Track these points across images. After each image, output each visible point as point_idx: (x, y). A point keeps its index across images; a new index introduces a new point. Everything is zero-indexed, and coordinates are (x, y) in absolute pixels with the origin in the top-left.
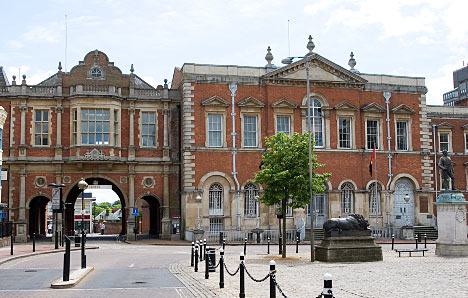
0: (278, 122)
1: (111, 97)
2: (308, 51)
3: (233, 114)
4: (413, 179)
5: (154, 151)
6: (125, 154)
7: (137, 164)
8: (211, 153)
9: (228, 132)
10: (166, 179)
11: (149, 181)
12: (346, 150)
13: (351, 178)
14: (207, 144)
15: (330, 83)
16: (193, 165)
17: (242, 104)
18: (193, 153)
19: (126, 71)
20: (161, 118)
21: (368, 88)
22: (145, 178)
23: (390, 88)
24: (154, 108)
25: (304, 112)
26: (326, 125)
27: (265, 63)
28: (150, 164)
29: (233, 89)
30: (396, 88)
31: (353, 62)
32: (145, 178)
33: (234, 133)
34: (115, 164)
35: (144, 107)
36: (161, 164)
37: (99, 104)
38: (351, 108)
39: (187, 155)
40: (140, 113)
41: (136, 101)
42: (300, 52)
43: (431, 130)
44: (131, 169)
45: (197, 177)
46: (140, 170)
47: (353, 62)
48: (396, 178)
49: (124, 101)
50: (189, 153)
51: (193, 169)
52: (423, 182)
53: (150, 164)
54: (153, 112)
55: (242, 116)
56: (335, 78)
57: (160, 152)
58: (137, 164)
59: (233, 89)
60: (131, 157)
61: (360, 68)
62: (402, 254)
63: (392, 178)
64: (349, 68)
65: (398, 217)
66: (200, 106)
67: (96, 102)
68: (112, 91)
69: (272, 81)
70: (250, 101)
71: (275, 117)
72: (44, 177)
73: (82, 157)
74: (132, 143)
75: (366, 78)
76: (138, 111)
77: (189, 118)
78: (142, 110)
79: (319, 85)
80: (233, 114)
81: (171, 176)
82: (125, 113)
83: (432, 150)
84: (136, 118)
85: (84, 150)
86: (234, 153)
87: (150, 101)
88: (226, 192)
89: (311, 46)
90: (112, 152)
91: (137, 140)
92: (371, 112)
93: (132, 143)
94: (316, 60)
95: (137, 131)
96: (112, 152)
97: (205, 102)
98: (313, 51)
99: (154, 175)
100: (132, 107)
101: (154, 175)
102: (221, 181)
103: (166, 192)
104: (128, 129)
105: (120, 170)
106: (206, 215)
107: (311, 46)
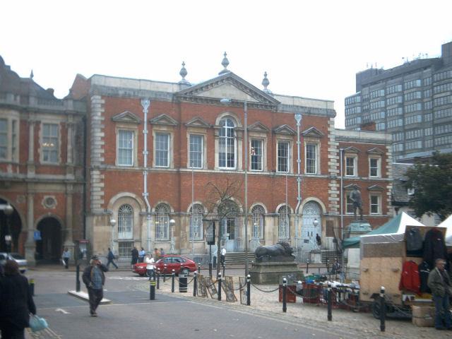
0: (191, 142)
1: (10, 107)
2: (222, 68)
3: (145, 131)
5: (57, 167)
6: (24, 169)
7: (37, 182)
8: (123, 173)
9: (140, 150)
10: (70, 200)
11: (50, 201)
12: (257, 172)
13: (262, 202)
16: (102, 185)
17: (155, 120)
18: (103, 171)
20: (64, 132)
21: (280, 109)
23: (301, 110)
24: (57, 120)
25: (217, 133)
26: (238, 147)
27: (179, 79)
28: (53, 182)
29: (146, 105)
30: (306, 111)
31: (266, 83)
32: (46, 197)
33: (145, 152)
35: (46, 119)
36: (64, 183)
38: (264, 130)
39: (96, 175)
40: (41, 126)
41: (37, 112)
42: (213, 72)
43: (338, 154)
45: (107, 198)
46: (41, 188)
47: (266, 83)
48: (304, 202)
49: (24, 111)
50: (98, 172)
52: (330, 205)
54: (57, 125)
55: (154, 135)
57: (63, 169)
59: (146, 105)
61: (276, 88)
63: (301, 201)
64: (262, 88)
65: (306, 241)
66: (111, 123)
69: (185, 98)
70: (162, 119)
71: (188, 137)
74: (31, 158)
75: (278, 99)
76: (38, 123)
77: (98, 135)
78: (43, 121)
79: (235, 104)
80: (145, 131)
81: (75, 196)
82: (25, 124)
83: (339, 174)
84: (37, 130)
86: (145, 174)
87: (52, 113)
88: (136, 214)
89: (225, 63)
90: (10, 170)
91: (37, 155)
92: (283, 134)
93: (31, 158)
94: (229, 79)
95: (37, 146)
96: (10, 170)
97: (116, 117)
98: (228, 68)
99: (56, 194)
100: (32, 118)
101: (56, 194)
102: (132, 203)
103: (69, 213)
105: (21, 188)
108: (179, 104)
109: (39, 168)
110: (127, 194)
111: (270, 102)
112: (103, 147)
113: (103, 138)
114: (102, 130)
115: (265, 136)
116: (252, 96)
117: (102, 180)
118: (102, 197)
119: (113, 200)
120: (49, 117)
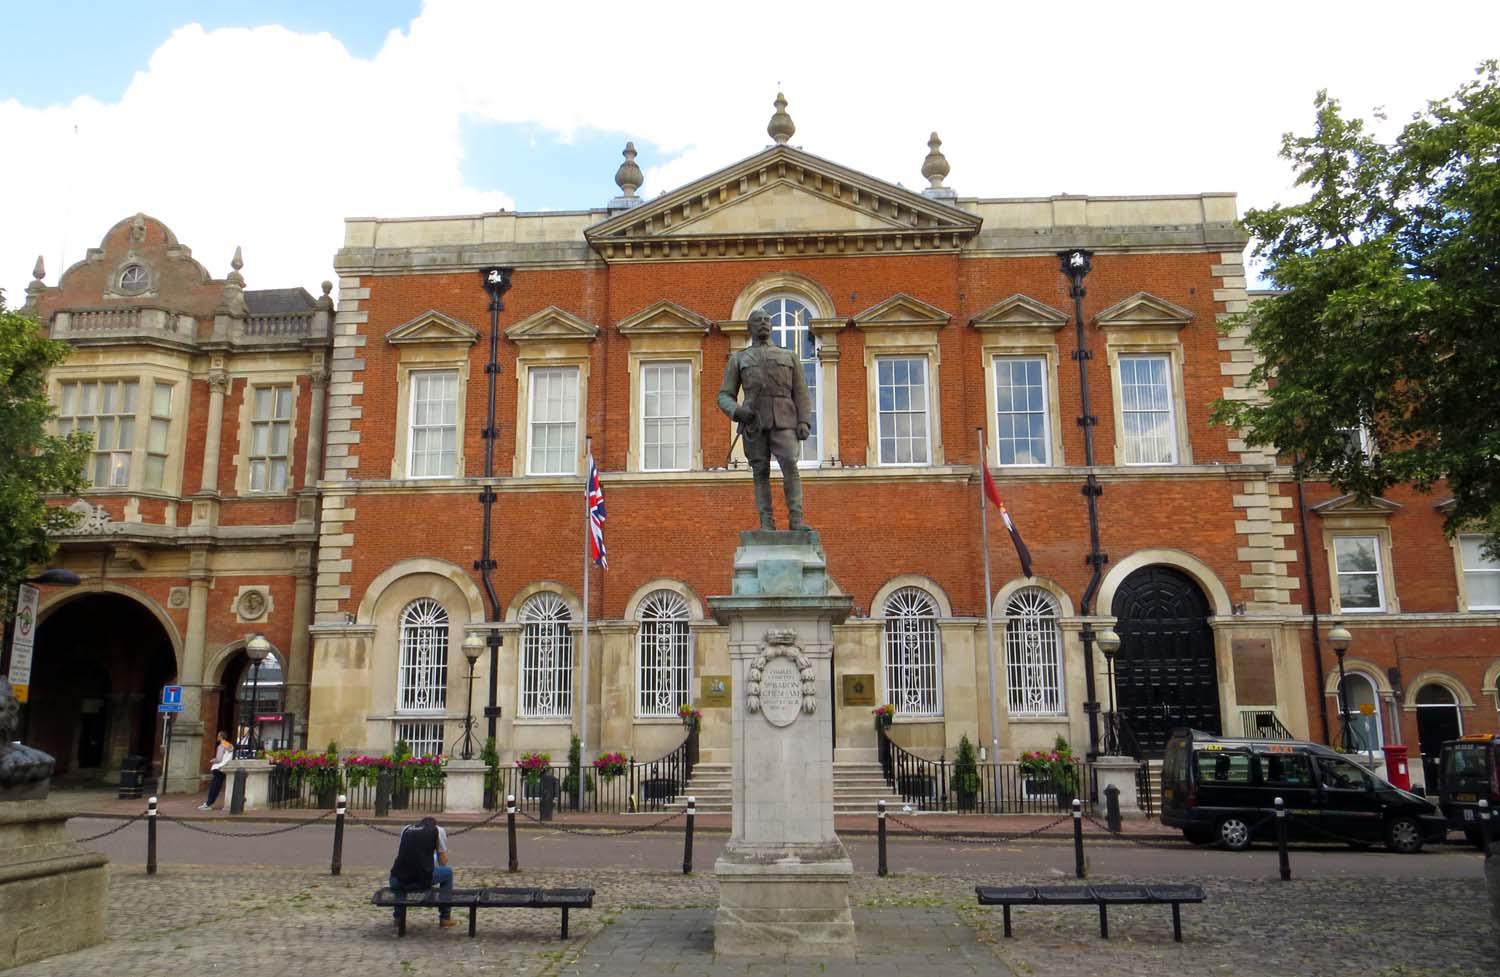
4: (424, 565)
5: (277, 501)
7: (214, 546)
13: (928, 575)
14: (397, 474)
15: (832, 239)
16: (348, 539)
19: (219, 271)
22: (243, 589)
27: (608, 194)
28: (258, 545)
31: (935, 168)
32: (243, 589)
34: (154, 549)
37: (109, 365)
40: (248, 392)
44: (198, 562)
45: (358, 581)
46: (229, 564)
47: (935, 168)
49: (196, 354)
51: (347, 552)
52: (1246, 580)
53: (258, 545)
54: (287, 386)
56: (861, 221)
58: (214, 546)
60: (202, 523)
61: (962, 183)
62: (1118, 915)
64: (918, 184)
67: (101, 359)
68: (153, 324)
69: (619, 248)
72: (264, 589)
73: (182, 532)
74: (209, 481)
75: (973, 210)
76: (239, 384)
78: (253, 379)
79: (802, 245)
82: (201, 391)
84: (231, 404)
85: (114, 502)
89: (781, 127)
90: (132, 513)
91: (227, 472)
92: (1009, 330)
93: (209, 481)
95: (229, 444)
96: (132, 513)
99: (270, 581)
100: (215, 369)
101: (270, 581)
102: (436, 591)
104: (203, 438)
105: (167, 568)
106: (378, 712)
107: (781, 127)
108: (606, 268)
109: (226, 503)
110: (424, 565)
111: (940, 222)
112: (355, 423)
113: (357, 400)
114: (357, 376)
115: (929, 340)
116: (874, 215)
117: (347, 526)
118: (345, 579)
119: (374, 590)
120: (269, 364)
